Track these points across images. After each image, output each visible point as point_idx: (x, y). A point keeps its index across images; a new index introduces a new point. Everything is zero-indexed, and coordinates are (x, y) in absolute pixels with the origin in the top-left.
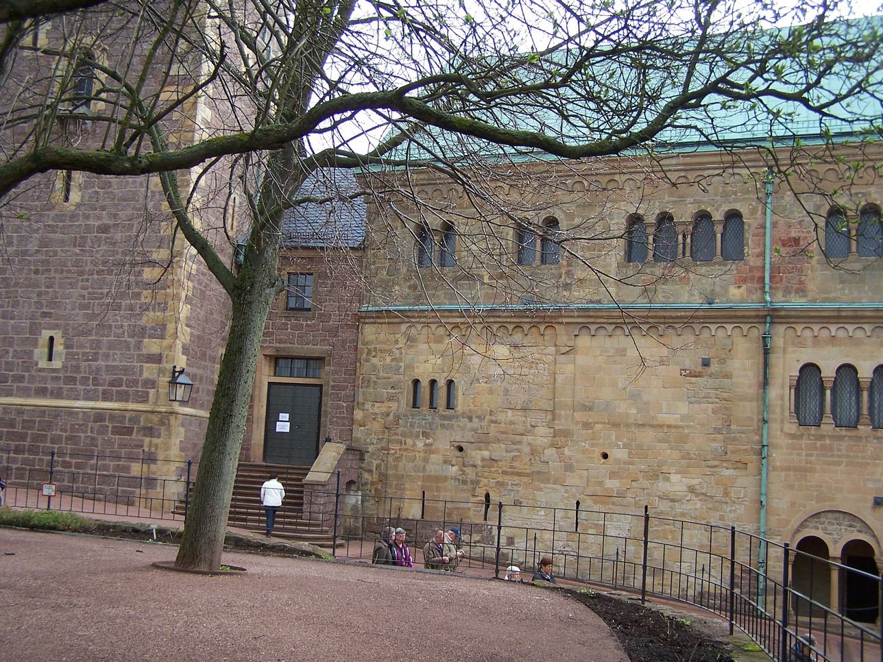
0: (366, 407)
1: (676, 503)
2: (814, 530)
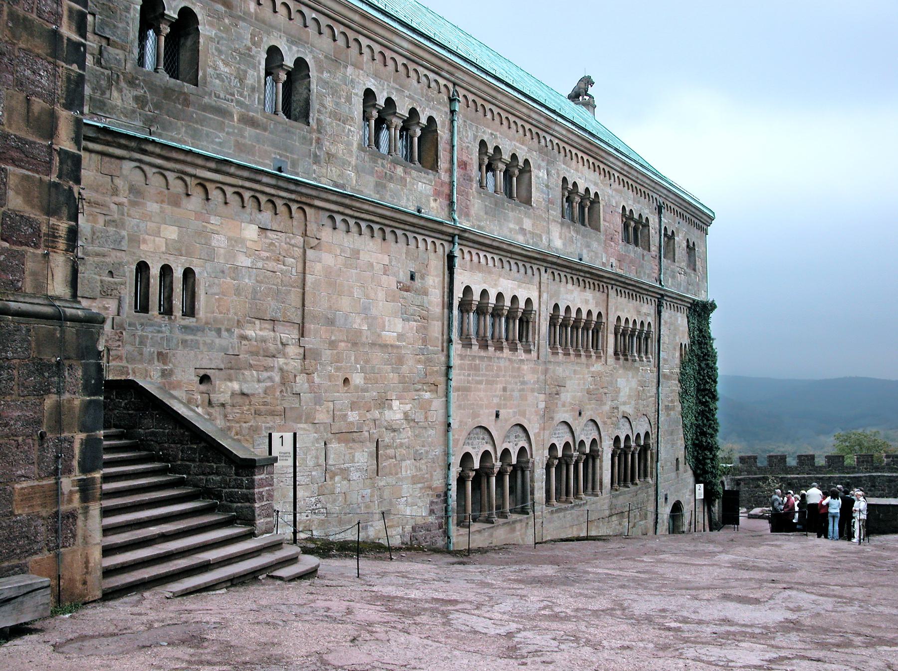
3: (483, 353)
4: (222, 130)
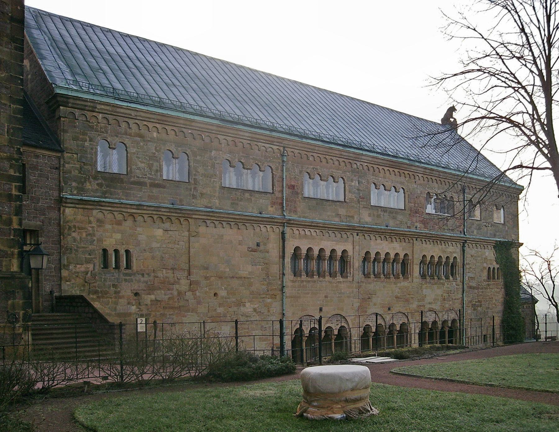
0: (71, 267)
3: (309, 279)
4: (141, 191)
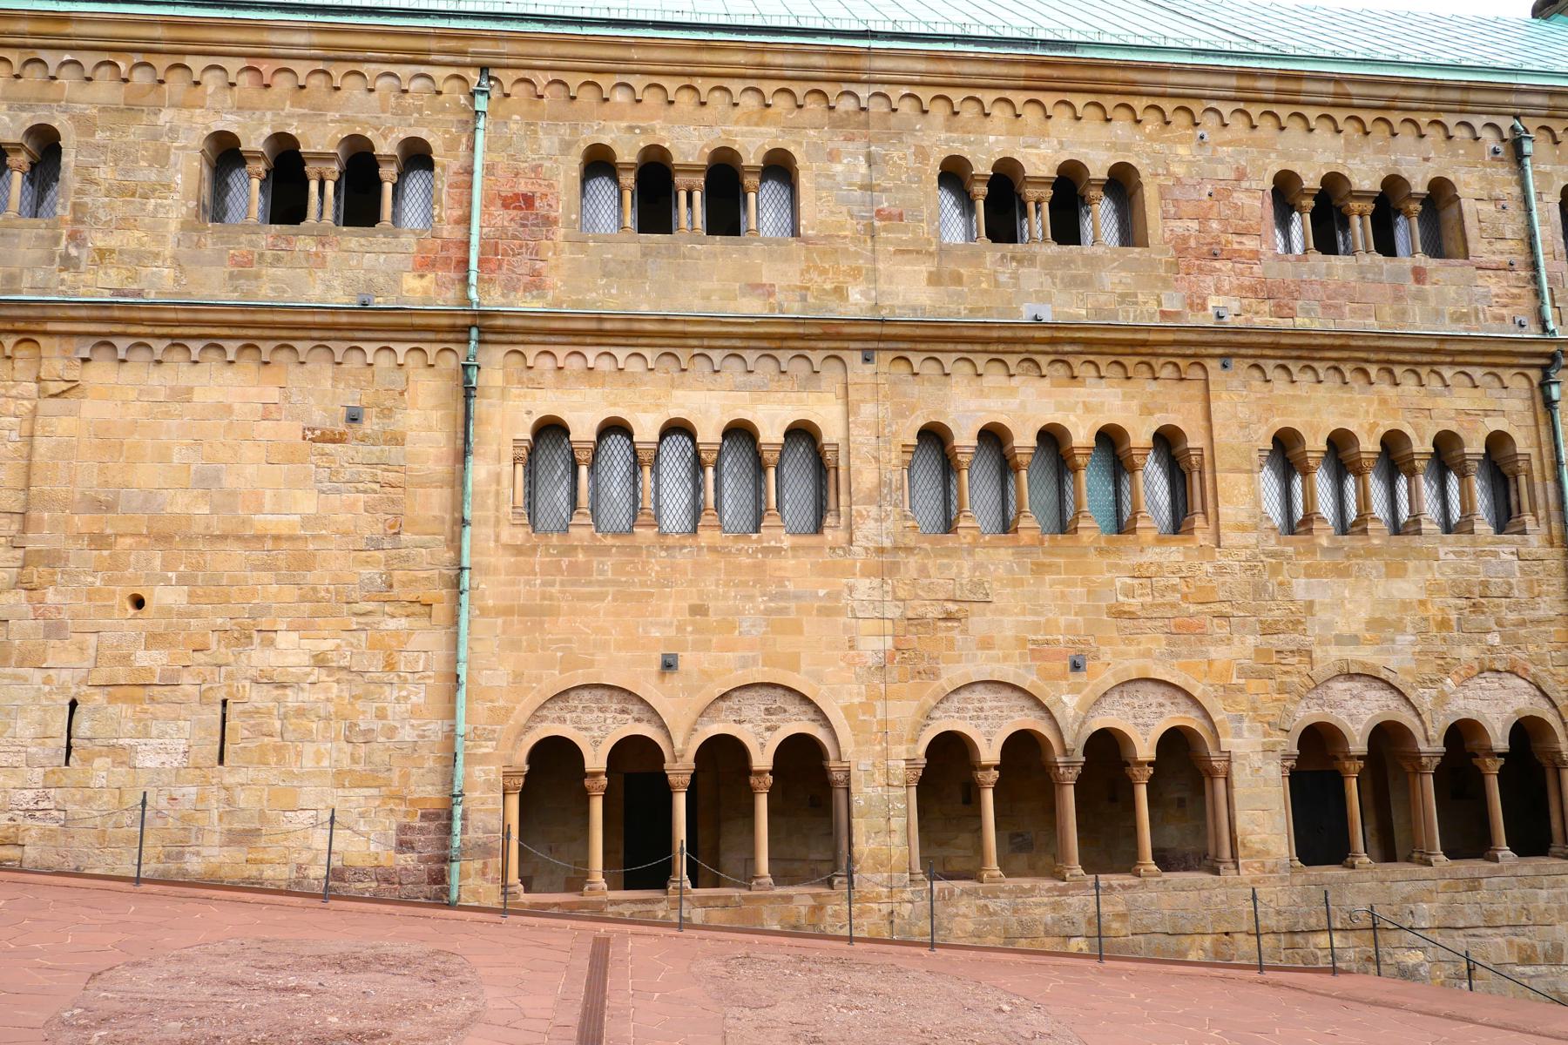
1: (288, 692)
2: (557, 725)
